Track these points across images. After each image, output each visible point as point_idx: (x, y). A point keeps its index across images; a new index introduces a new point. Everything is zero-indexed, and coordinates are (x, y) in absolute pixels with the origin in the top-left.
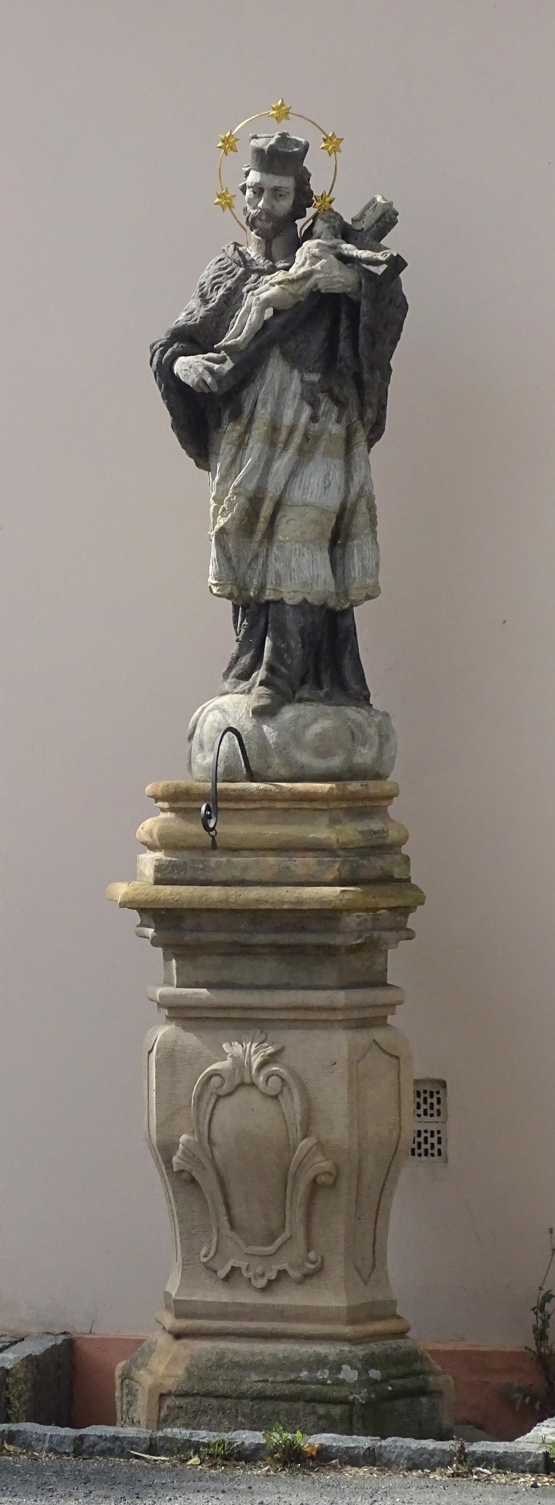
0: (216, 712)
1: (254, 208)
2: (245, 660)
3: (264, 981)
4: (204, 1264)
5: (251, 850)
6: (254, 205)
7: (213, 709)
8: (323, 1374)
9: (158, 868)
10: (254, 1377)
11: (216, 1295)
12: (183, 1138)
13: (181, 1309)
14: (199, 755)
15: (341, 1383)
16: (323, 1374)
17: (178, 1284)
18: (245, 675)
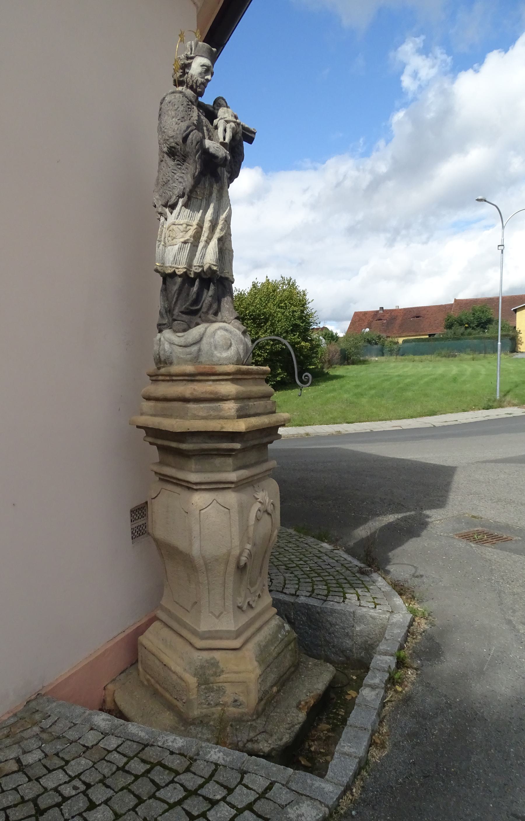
0: (221, 330)
1: (202, 78)
2: (215, 306)
3: (253, 462)
4: (239, 607)
5: (255, 398)
6: (203, 76)
7: (218, 329)
8: (283, 632)
9: (238, 410)
10: (273, 648)
11: (244, 619)
12: (249, 546)
13: (238, 634)
14: (215, 352)
15: (288, 632)
16: (283, 632)
17: (232, 621)
18: (216, 314)
